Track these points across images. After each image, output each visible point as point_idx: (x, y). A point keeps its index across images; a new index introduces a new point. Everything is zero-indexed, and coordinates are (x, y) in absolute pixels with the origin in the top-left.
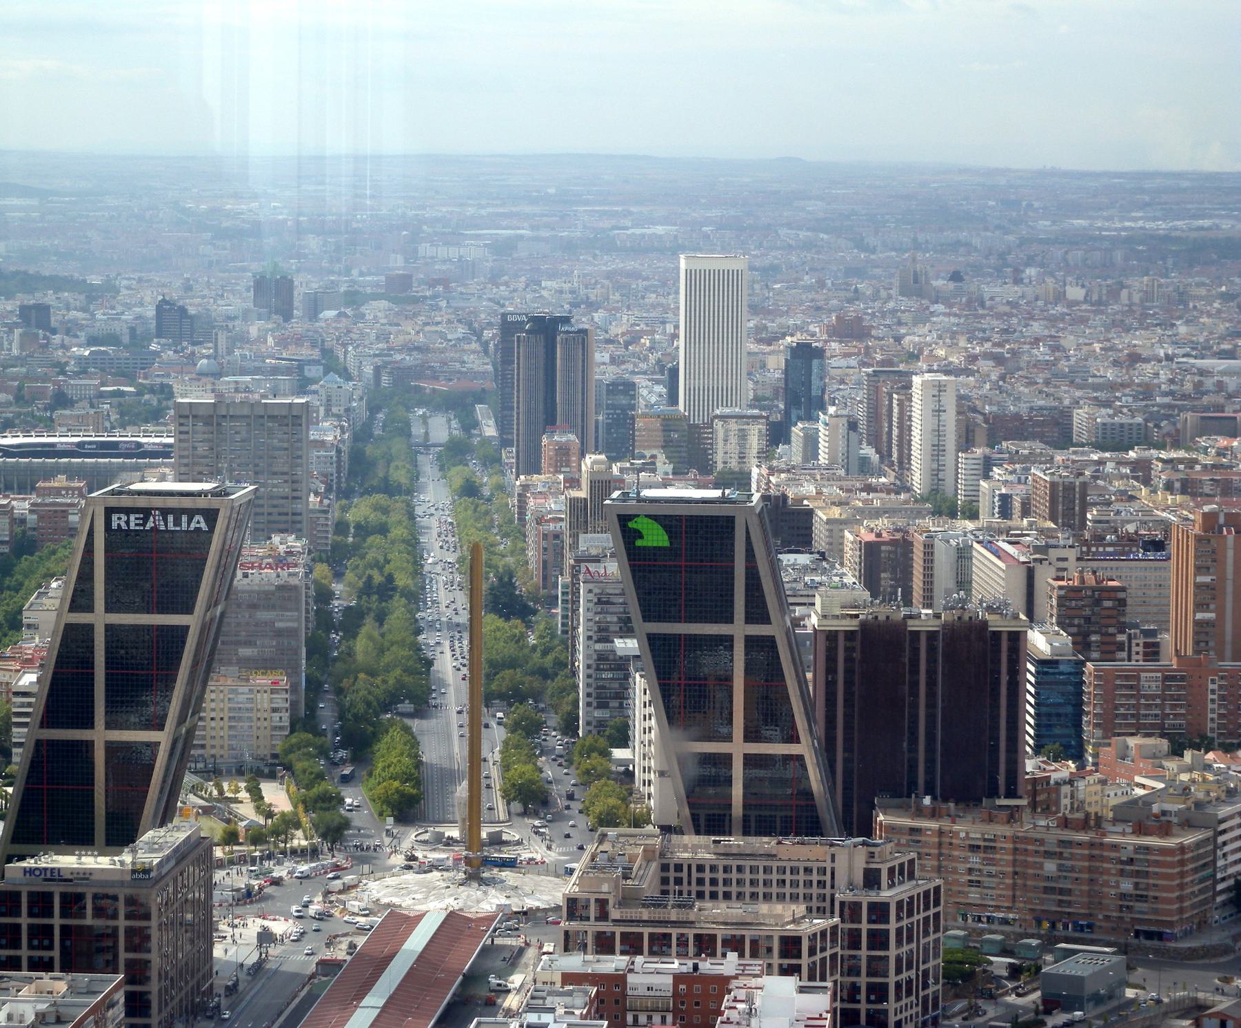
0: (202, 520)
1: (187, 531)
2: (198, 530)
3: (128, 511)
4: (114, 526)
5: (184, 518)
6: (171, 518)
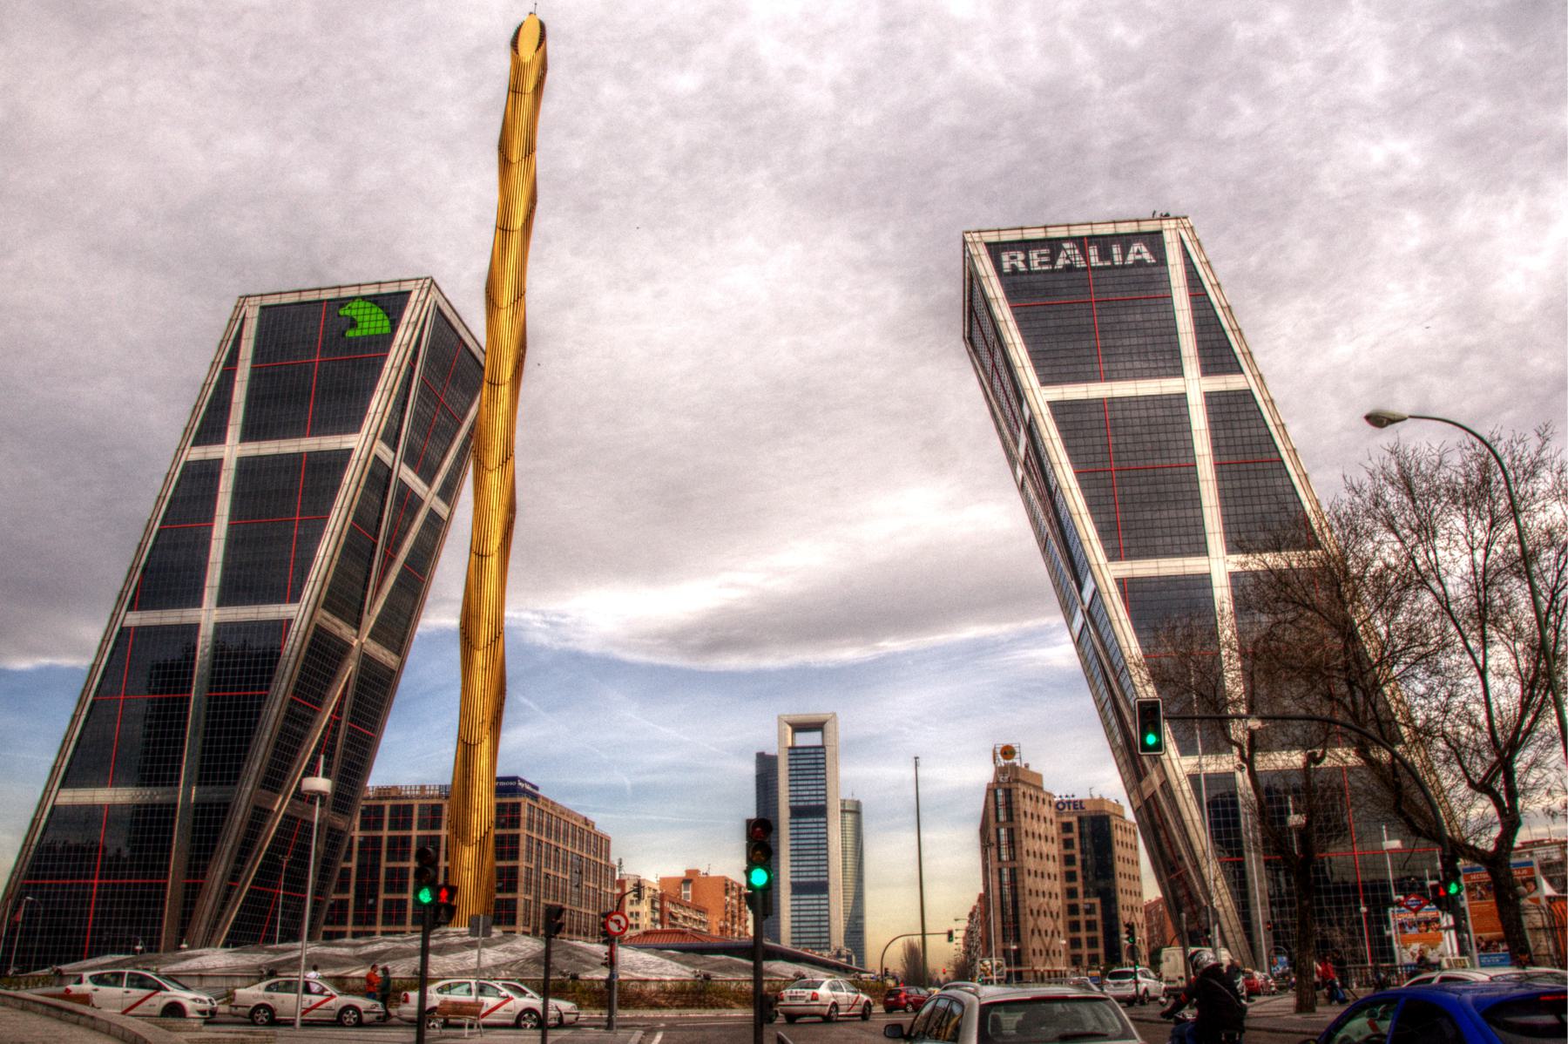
0: (1144, 249)
1: (1123, 267)
2: (1140, 263)
3: (1026, 245)
4: (1006, 266)
5: (1116, 250)
6: (1093, 251)
